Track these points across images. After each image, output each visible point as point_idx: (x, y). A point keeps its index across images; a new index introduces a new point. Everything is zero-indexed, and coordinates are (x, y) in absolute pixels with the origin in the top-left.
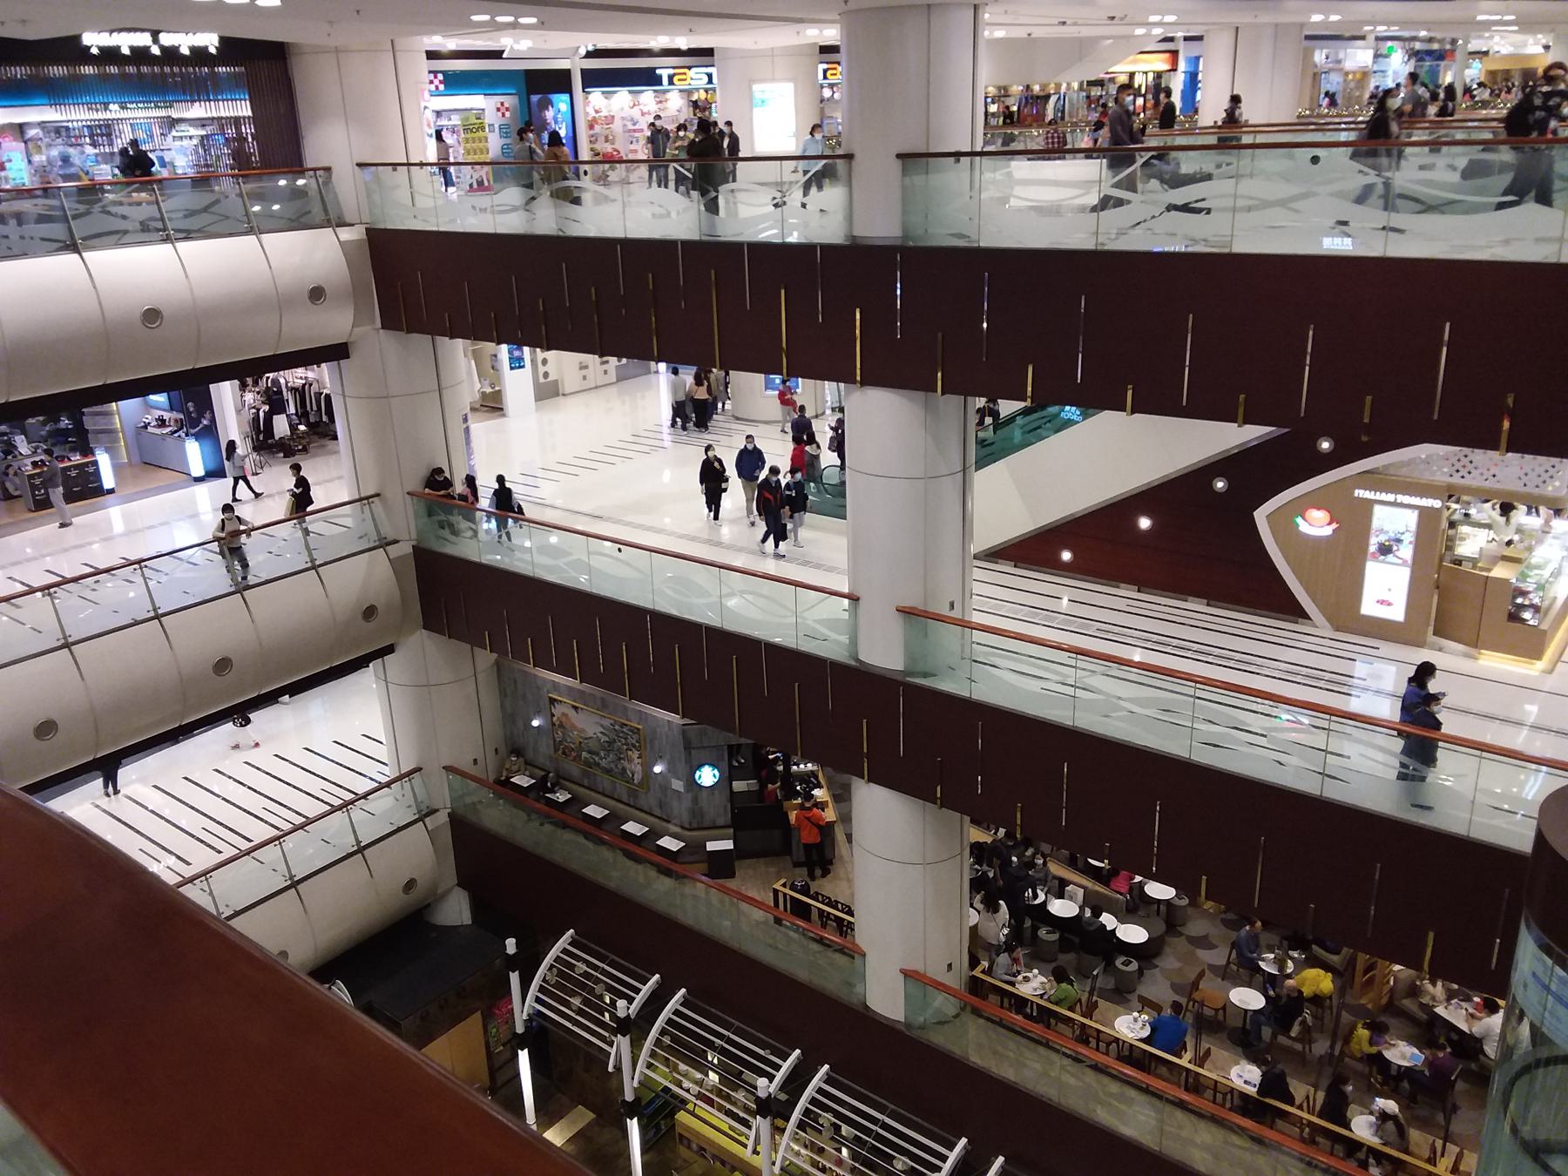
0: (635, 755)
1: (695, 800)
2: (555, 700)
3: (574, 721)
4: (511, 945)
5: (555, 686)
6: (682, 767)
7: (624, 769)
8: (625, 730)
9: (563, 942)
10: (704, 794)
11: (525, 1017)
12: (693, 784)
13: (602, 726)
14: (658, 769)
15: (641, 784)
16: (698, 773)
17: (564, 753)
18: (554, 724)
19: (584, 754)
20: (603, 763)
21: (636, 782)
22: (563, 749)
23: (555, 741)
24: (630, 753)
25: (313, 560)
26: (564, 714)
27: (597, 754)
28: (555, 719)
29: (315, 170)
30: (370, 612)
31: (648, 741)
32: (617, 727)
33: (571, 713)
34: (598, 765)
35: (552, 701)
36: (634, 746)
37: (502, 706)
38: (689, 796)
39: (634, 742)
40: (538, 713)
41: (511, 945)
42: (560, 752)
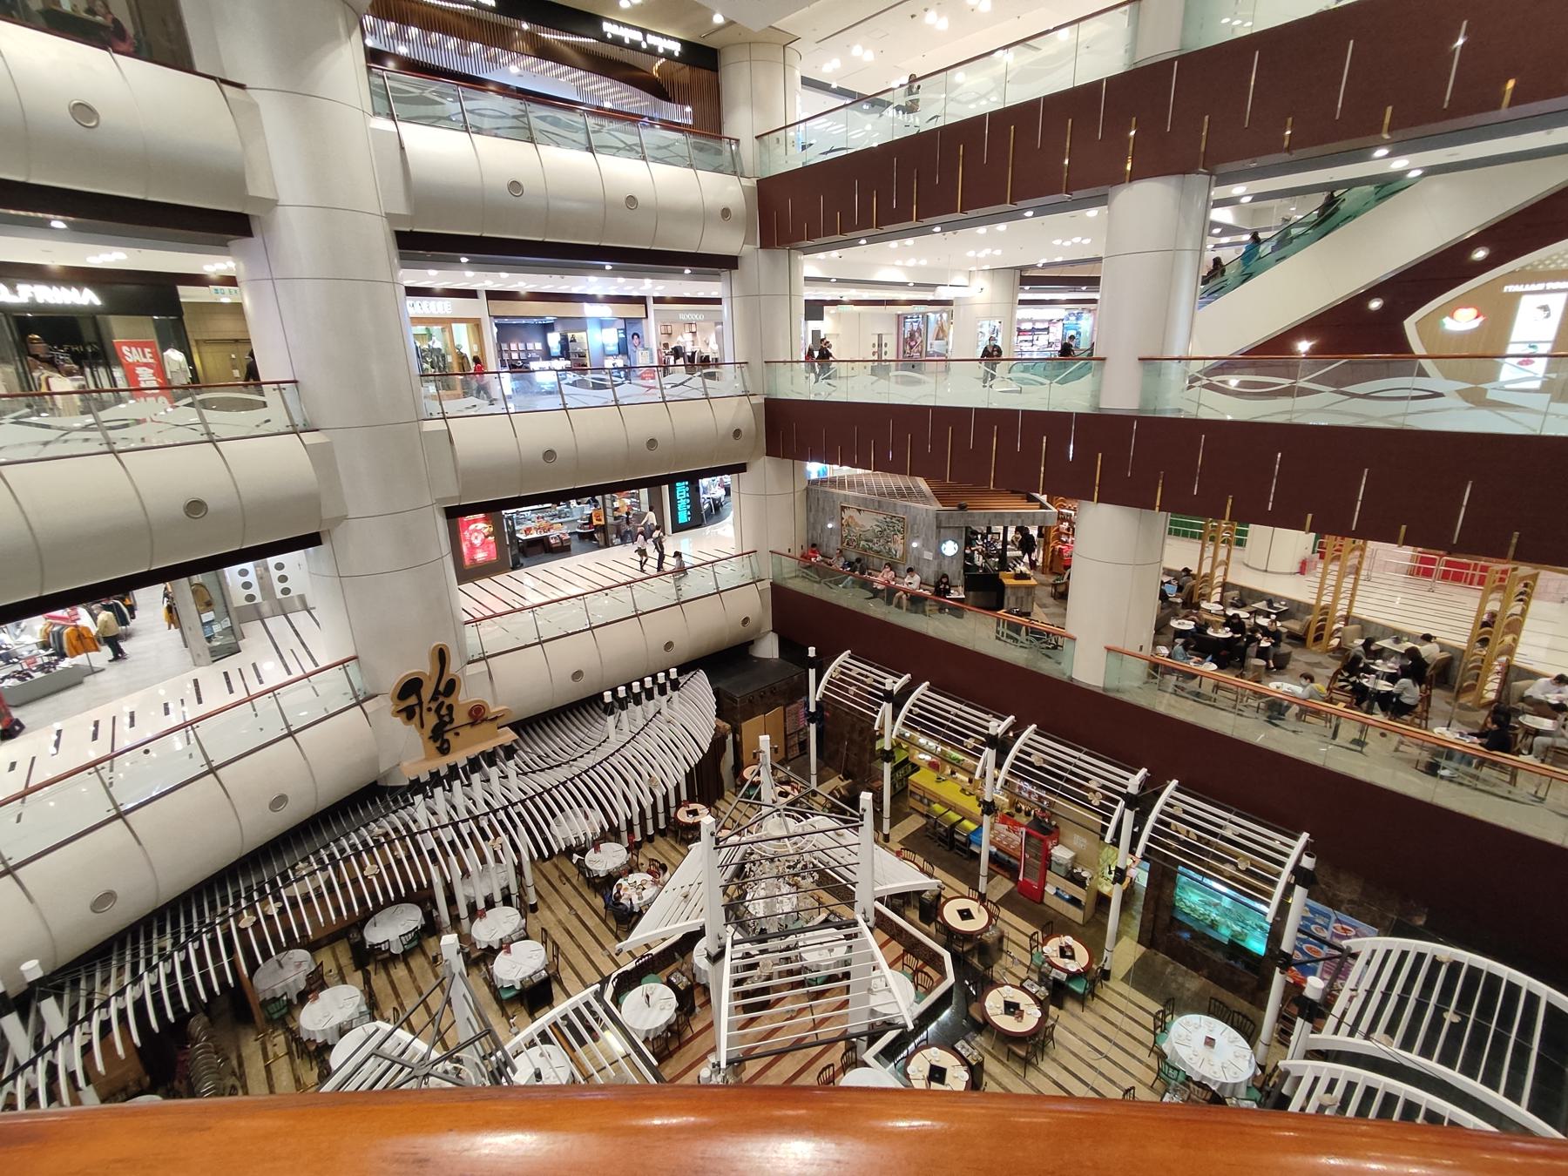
1: (940, 565)
4: (812, 652)
5: (846, 498)
6: (933, 541)
9: (845, 655)
10: (946, 562)
11: (817, 699)
12: (939, 554)
14: (915, 545)
19: (862, 543)
20: (875, 547)
22: (847, 542)
25: (707, 394)
26: (851, 517)
27: (871, 541)
29: (730, 139)
30: (737, 433)
32: (888, 520)
34: (871, 549)
35: (843, 508)
37: (807, 519)
38: (936, 562)
40: (831, 520)
41: (812, 652)
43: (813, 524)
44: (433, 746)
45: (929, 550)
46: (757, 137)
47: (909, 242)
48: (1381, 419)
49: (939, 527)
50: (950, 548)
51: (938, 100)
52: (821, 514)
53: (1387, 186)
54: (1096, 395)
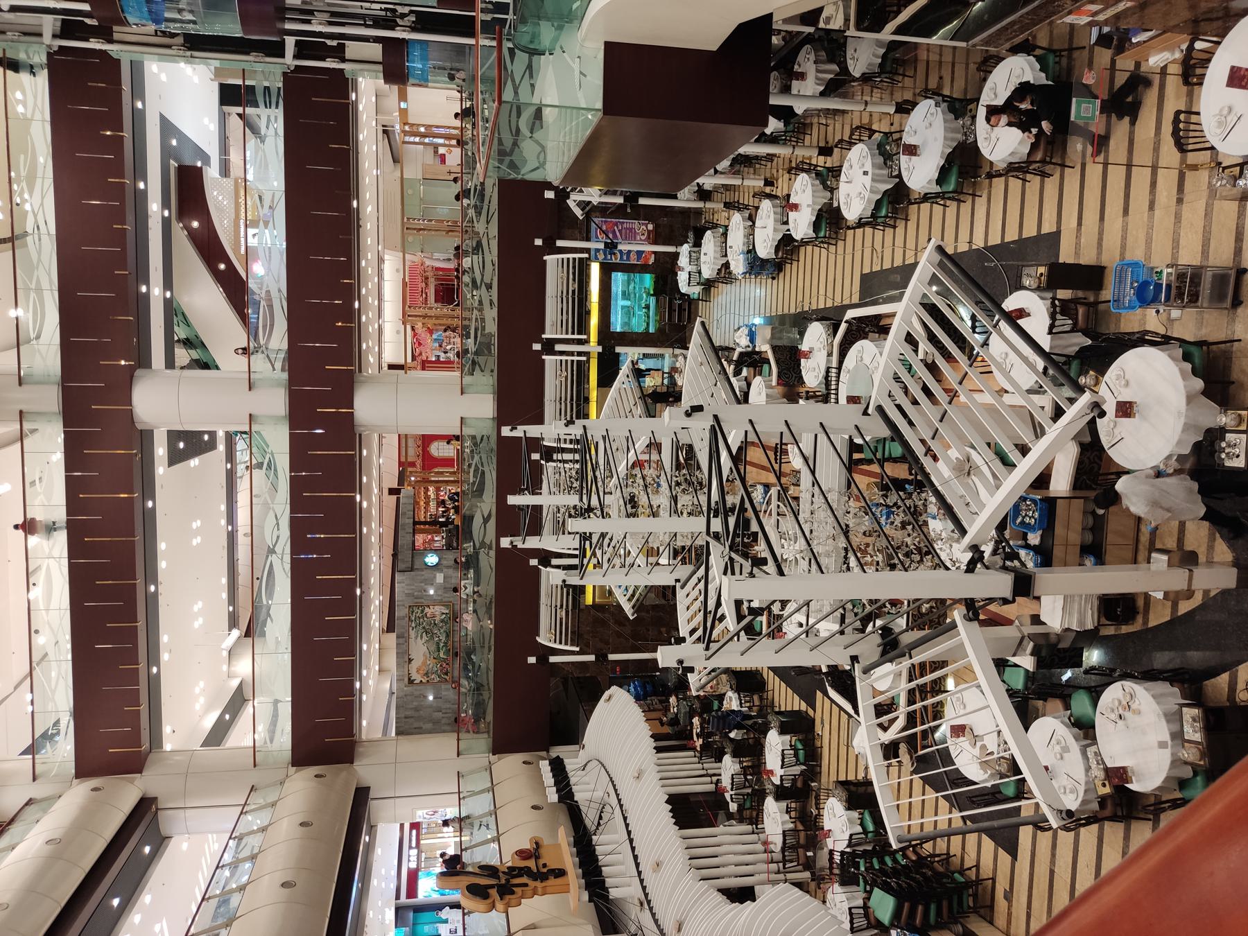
0: (427, 610)
2: (409, 679)
3: (420, 663)
4: (532, 660)
6: (426, 574)
7: (442, 621)
9: (539, 640)
13: (416, 638)
14: (432, 592)
15: (447, 606)
16: (429, 564)
17: (446, 674)
20: (444, 639)
21: (447, 612)
23: (439, 681)
27: (438, 644)
28: (424, 681)
31: (416, 600)
32: (413, 625)
34: (445, 643)
36: (422, 611)
38: (445, 570)
39: (419, 611)
40: (425, 697)
42: (446, 677)
43: (436, 728)
44: (552, 881)
45: (435, 577)
46: (34, 779)
47: (164, 639)
48: (282, 256)
49: (412, 569)
50: (432, 559)
51: (48, 565)
52: (421, 712)
53: (172, 311)
54: (276, 419)
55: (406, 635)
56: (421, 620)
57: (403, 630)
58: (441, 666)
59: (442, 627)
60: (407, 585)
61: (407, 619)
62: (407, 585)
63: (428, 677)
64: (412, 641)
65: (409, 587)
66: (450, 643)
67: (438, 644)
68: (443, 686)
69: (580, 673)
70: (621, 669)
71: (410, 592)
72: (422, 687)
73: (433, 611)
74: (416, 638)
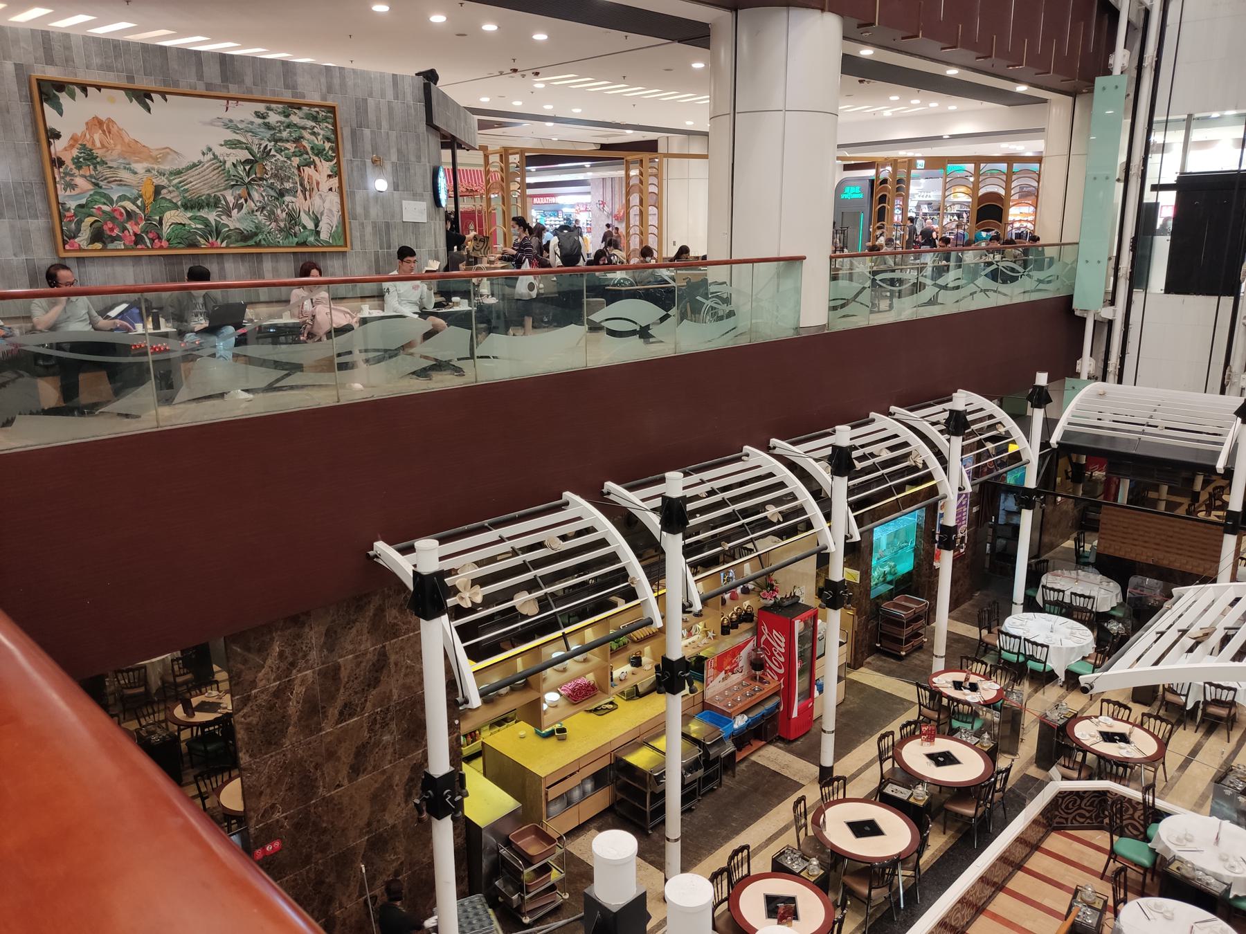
0: (325, 167)
2: (61, 86)
3: (133, 134)
7: (293, 218)
8: (294, 119)
13: (230, 125)
17: (98, 236)
18: (58, 162)
20: (236, 221)
21: (324, 236)
24: (308, 171)
27: (213, 203)
28: (58, 146)
32: (273, 118)
33: (124, 112)
36: (319, 152)
39: (319, 142)
42: (83, 239)
55: (234, 90)
56: (291, 147)
57: (248, 80)
58: (130, 215)
59: (272, 216)
60: (390, 109)
61: (288, 97)
62: (390, 109)
63: (78, 163)
64: (215, 109)
65: (385, 110)
66: (222, 246)
67: (213, 203)
68: (37, 225)
69: (249, 728)
70: (276, 853)
71: (372, 116)
72: (24, 138)
73: (325, 186)
74: (230, 125)
